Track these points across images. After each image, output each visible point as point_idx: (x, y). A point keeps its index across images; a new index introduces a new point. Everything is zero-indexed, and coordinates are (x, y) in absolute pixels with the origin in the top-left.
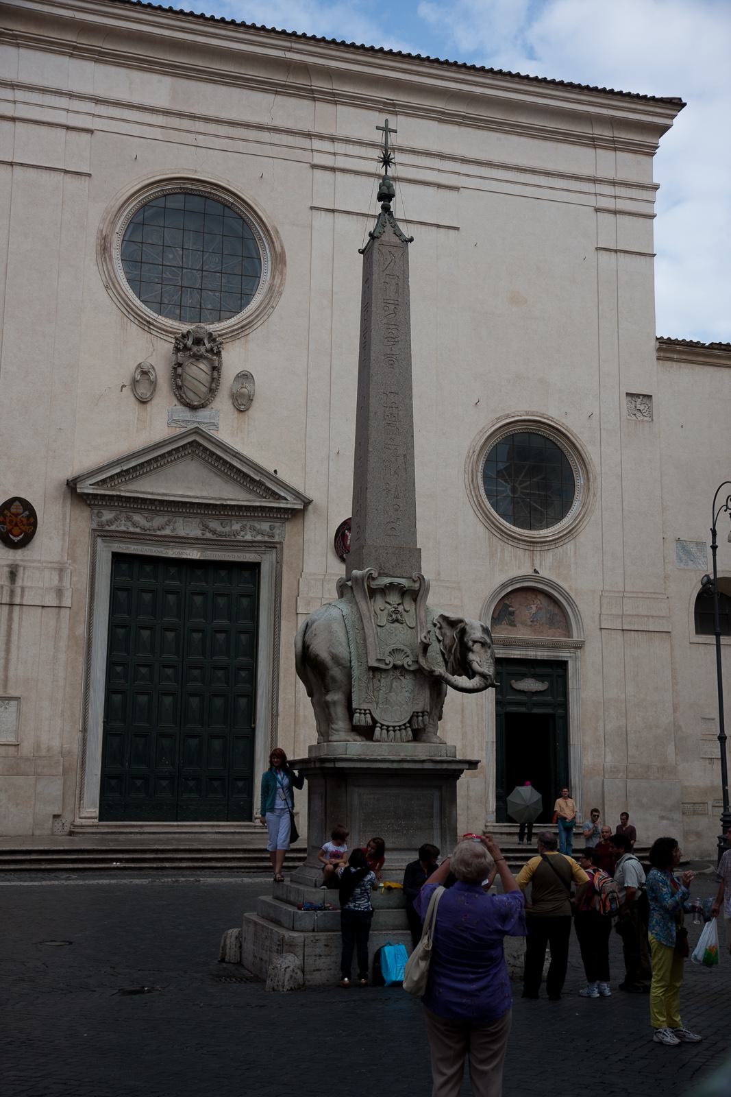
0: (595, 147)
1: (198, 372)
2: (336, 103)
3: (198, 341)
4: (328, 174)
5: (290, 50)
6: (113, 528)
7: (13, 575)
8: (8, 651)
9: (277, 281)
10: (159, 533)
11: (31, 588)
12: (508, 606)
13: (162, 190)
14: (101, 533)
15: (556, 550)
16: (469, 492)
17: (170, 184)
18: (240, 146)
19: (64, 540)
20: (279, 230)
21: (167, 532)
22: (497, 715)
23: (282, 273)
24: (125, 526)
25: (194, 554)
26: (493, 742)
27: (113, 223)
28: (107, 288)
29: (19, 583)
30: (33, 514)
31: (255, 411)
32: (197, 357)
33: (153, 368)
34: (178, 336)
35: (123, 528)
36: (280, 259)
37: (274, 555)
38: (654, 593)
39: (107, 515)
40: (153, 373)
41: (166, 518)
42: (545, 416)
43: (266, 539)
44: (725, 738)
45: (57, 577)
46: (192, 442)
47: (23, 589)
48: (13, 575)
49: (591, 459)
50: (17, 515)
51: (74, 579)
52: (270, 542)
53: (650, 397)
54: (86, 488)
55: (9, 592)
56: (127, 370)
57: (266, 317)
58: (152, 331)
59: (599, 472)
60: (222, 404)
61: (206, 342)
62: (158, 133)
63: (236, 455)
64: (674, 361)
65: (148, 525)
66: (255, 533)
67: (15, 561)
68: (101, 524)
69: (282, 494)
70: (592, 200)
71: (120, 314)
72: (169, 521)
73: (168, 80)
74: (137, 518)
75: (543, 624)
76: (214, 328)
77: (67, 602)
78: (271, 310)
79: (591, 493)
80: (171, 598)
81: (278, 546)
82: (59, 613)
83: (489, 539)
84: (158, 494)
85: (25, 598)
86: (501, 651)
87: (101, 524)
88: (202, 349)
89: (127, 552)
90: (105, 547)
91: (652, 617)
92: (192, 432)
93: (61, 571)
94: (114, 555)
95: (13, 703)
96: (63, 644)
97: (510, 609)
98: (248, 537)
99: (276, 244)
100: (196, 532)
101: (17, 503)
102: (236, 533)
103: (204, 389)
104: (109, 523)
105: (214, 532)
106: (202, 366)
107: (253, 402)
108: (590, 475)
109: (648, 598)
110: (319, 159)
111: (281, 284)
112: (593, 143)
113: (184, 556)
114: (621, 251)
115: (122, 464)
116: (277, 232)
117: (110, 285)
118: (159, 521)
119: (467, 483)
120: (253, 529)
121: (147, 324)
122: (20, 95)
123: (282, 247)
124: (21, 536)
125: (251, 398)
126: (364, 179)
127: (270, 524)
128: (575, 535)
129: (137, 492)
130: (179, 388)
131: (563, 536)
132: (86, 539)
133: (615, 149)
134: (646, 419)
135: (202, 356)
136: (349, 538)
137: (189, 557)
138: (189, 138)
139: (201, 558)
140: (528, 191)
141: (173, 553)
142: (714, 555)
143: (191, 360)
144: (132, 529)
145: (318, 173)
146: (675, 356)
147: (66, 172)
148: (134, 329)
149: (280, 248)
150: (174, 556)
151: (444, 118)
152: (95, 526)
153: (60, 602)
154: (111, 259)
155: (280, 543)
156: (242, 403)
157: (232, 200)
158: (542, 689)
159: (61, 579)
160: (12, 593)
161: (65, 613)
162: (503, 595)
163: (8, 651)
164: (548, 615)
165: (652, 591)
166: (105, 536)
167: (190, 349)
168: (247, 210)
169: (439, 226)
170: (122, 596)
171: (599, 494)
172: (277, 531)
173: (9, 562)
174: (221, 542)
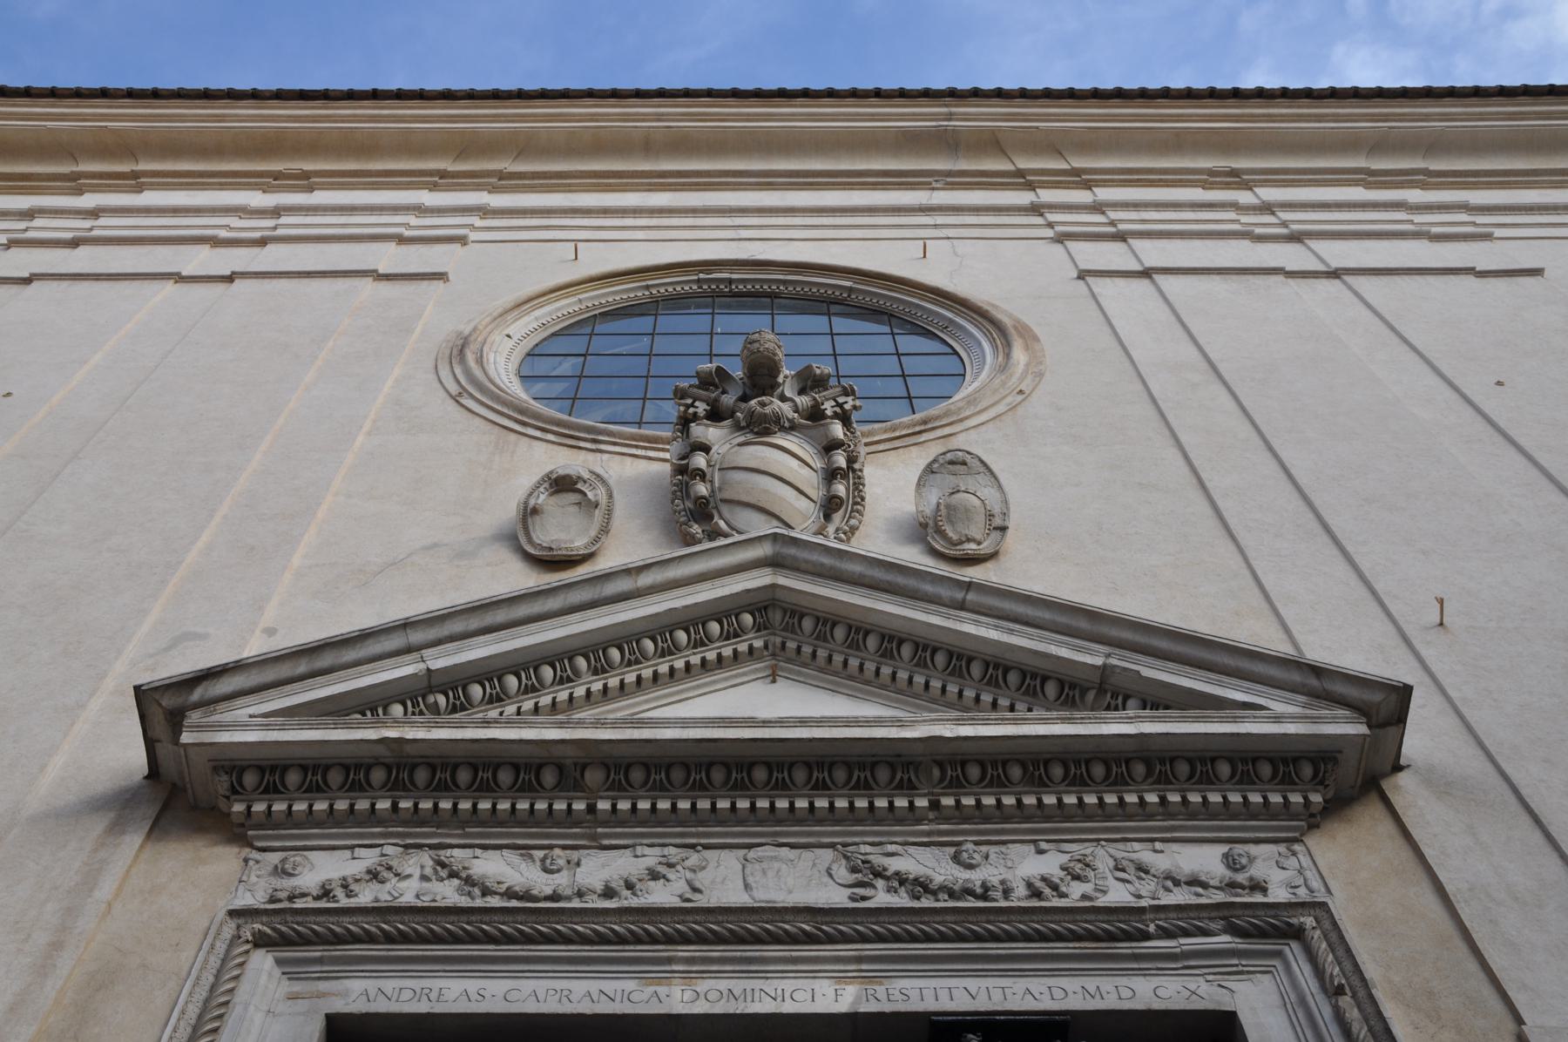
5: (950, 117)
13: (647, 287)
19: (43, 968)
21: (661, 895)
34: (684, 384)
41: (651, 857)
58: (603, 447)
71: (489, 426)
81: (1309, 921)
89: (422, 1007)
105: (921, 886)
107: (1010, 532)
115: (426, 653)
125: (998, 522)
137: (788, 1008)
139: (865, 1008)
150: (701, 1008)
166: (303, 941)
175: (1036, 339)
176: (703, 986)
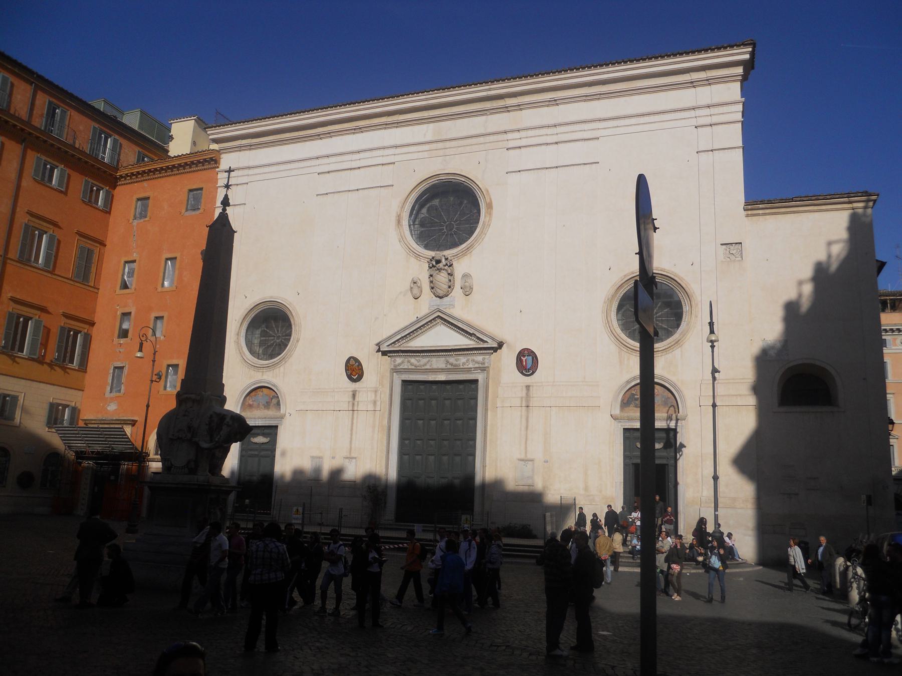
0: (694, 87)
1: (442, 278)
2: (521, 110)
3: (438, 262)
4: (518, 151)
5: (490, 90)
6: (401, 367)
7: (354, 396)
8: (351, 434)
9: (487, 219)
10: (423, 368)
11: (362, 401)
12: (633, 395)
14: (395, 370)
15: (667, 356)
16: (605, 325)
17: (431, 180)
18: (468, 149)
20: (489, 191)
21: (428, 367)
22: (625, 465)
23: (490, 214)
24: (407, 365)
25: (442, 377)
26: (621, 482)
27: (403, 207)
28: (400, 241)
29: (357, 399)
30: (360, 364)
31: (475, 295)
32: (439, 270)
33: (420, 280)
35: (406, 367)
36: (490, 206)
37: (485, 375)
38: (742, 379)
39: (399, 360)
40: (419, 282)
41: (427, 359)
42: (659, 269)
43: (481, 366)
44: (718, 478)
45: (374, 396)
46: (437, 317)
47: (358, 404)
48: (354, 396)
49: (694, 293)
50: (353, 365)
51: (382, 396)
52: (483, 367)
53: (741, 243)
54: (384, 348)
55: (352, 404)
56: (407, 284)
57: (481, 240)
59: (699, 299)
60: (457, 292)
61: (443, 260)
62: (426, 154)
63: (458, 320)
64: (760, 216)
65: (418, 364)
66: (474, 363)
67: (355, 388)
68: (395, 366)
69: (485, 339)
70: (694, 122)
72: (429, 361)
73: (431, 125)
74: (413, 360)
75: (659, 405)
76: (448, 253)
77: (378, 408)
78: (484, 236)
79: (693, 316)
80: (433, 402)
82: (375, 413)
83: (619, 353)
84: (419, 347)
85: (359, 407)
86: (627, 424)
87: (395, 366)
88: (441, 265)
90: (398, 377)
91: (740, 395)
92: (436, 311)
93: (376, 392)
94: (403, 381)
95: (354, 460)
96: (376, 429)
97: (636, 396)
98: (471, 366)
99: (486, 198)
100: (443, 366)
101: (352, 359)
102: (464, 364)
103: (446, 287)
104: (399, 364)
106: (442, 274)
108: (693, 303)
109: (738, 383)
110: (511, 144)
111: (490, 220)
112: (693, 84)
113: (437, 379)
114: (715, 150)
116: (488, 191)
117: (402, 239)
118: (424, 361)
119: (604, 320)
120: (473, 361)
121: (418, 256)
122: (362, 155)
123: (491, 199)
124: (357, 376)
126: (538, 148)
127: (482, 357)
128: (682, 343)
129: (409, 347)
130: (432, 288)
131: (672, 346)
132: (388, 374)
133: (710, 84)
134: (737, 259)
135: (441, 269)
136: (524, 361)
137: (439, 380)
138: (441, 152)
140: (647, 127)
141: (431, 378)
142: (713, 352)
143: (438, 271)
144: (410, 367)
145: (511, 151)
146: (761, 212)
147: (381, 187)
148: (413, 260)
149: (489, 200)
151: (587, 98)
152: (392, 367)
153: (375, 407)
154: (402, 226)
155: (488, 367)
156: (467, 291)
157: (463, 180)
158: (659, 448)
159: (376, 396)
160: (353, 404)
161: (378, 413)
162: (628, 388)
163: (351, 434)
164: (663, 399)
165: (741, 378)
167: (435, 267)
168: (472, 183)
169: (585, 164)
170: (409, 402)
171: (699, 316)
172: (486, 361)
173: (353, 389)
174: (456, 369)
175: (492, 209)
176: (432, 376)
